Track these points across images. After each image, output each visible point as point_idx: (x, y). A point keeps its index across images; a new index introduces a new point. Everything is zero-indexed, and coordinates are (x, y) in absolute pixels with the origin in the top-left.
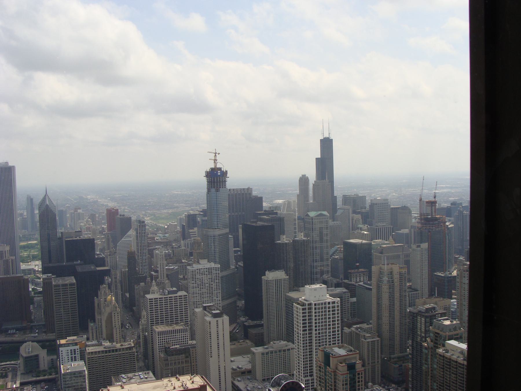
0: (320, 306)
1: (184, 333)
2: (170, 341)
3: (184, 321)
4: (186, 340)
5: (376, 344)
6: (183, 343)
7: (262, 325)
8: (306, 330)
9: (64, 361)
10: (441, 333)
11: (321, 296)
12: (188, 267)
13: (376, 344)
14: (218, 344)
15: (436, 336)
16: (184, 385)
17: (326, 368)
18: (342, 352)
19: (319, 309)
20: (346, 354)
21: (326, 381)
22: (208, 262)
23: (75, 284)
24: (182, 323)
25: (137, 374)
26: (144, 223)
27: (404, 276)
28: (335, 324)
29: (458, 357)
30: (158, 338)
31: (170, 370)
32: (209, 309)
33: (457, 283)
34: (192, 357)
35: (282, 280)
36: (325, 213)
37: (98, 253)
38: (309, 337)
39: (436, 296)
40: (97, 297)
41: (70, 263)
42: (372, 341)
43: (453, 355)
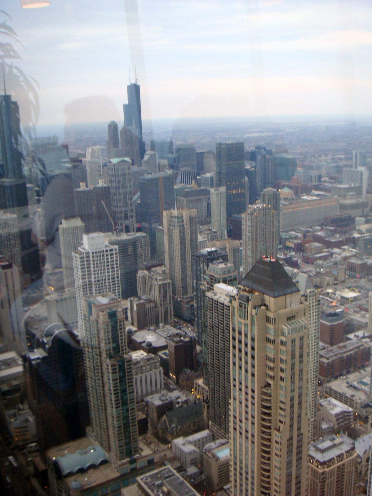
10: (215, 276)
13: (167, 286)
15: (212, 279)
17: (89, 316)
18: (104, 300)
20: (108, 302)
28: (112, 272)
29: (225, 299)
33: (242, 226)
36: (127, 159)
39: (226, 238)
42: (163, 284)
43: (220, 297)
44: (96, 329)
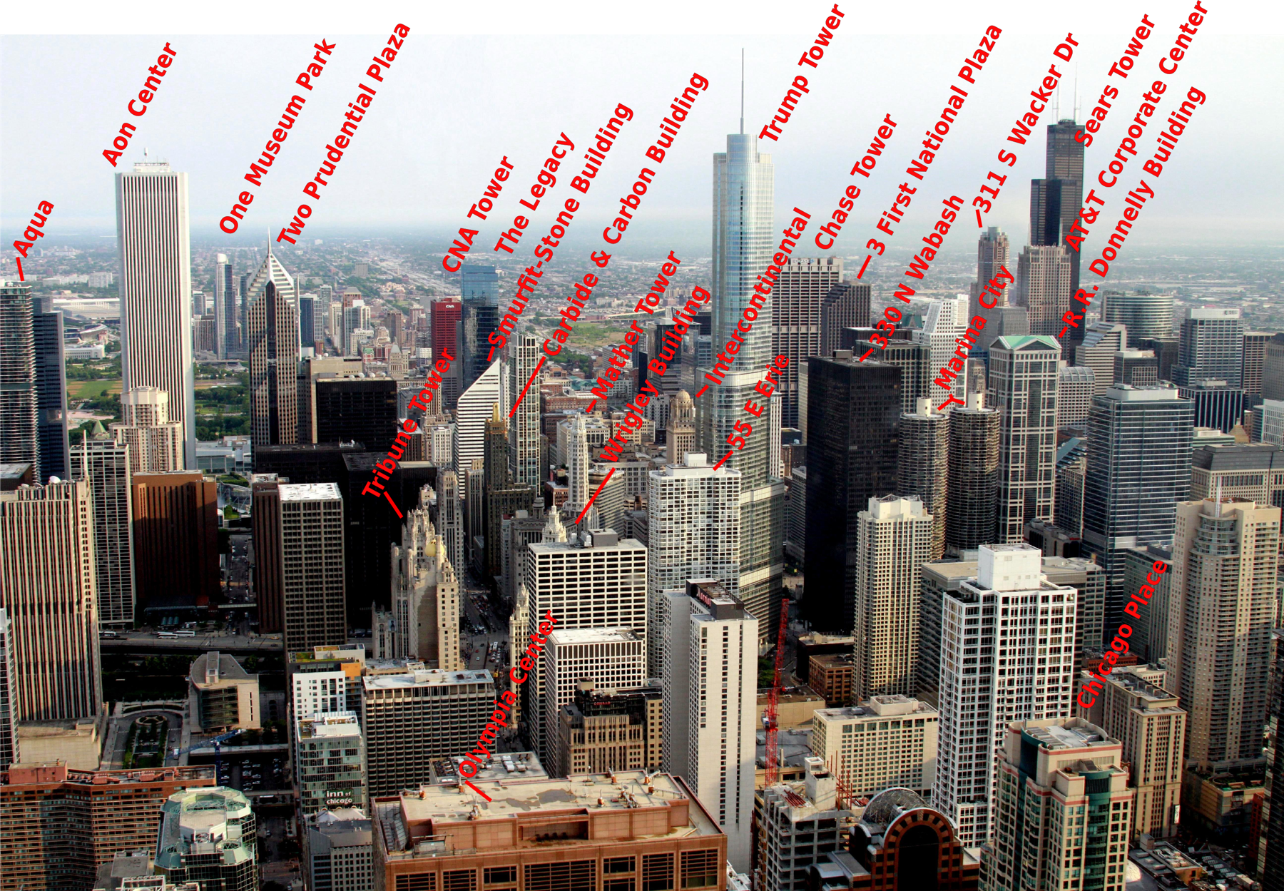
0: (1020, 606)
1: (631, 656)
2: (592, 674)
3: (633, 622)
4: (636, 674)
5: (1173, 725)
6: (626, 681)
7: (849, 648)
8: (974, 671)
9: (303, 709)
11: (1023, 577)
12: (651, 472)
13: (1173, 725)
14: (725, 691)
16: (627, 797)
19: (1015, 612)
21: (1020, 817)
22: (709, 461)
23: (339, 503)
24: (625, 628)
25: (496, 757)
26: (533, 344)
27: (1270, 537)
30: (560, 663)
31: (587, 755)
32: (705, 593)
34: (649, 721)
35: (914, 525)
37: (403, 420)
38: (980, 690)
40: (399, 544)
41: (327, 448)
44: (1041, 818)
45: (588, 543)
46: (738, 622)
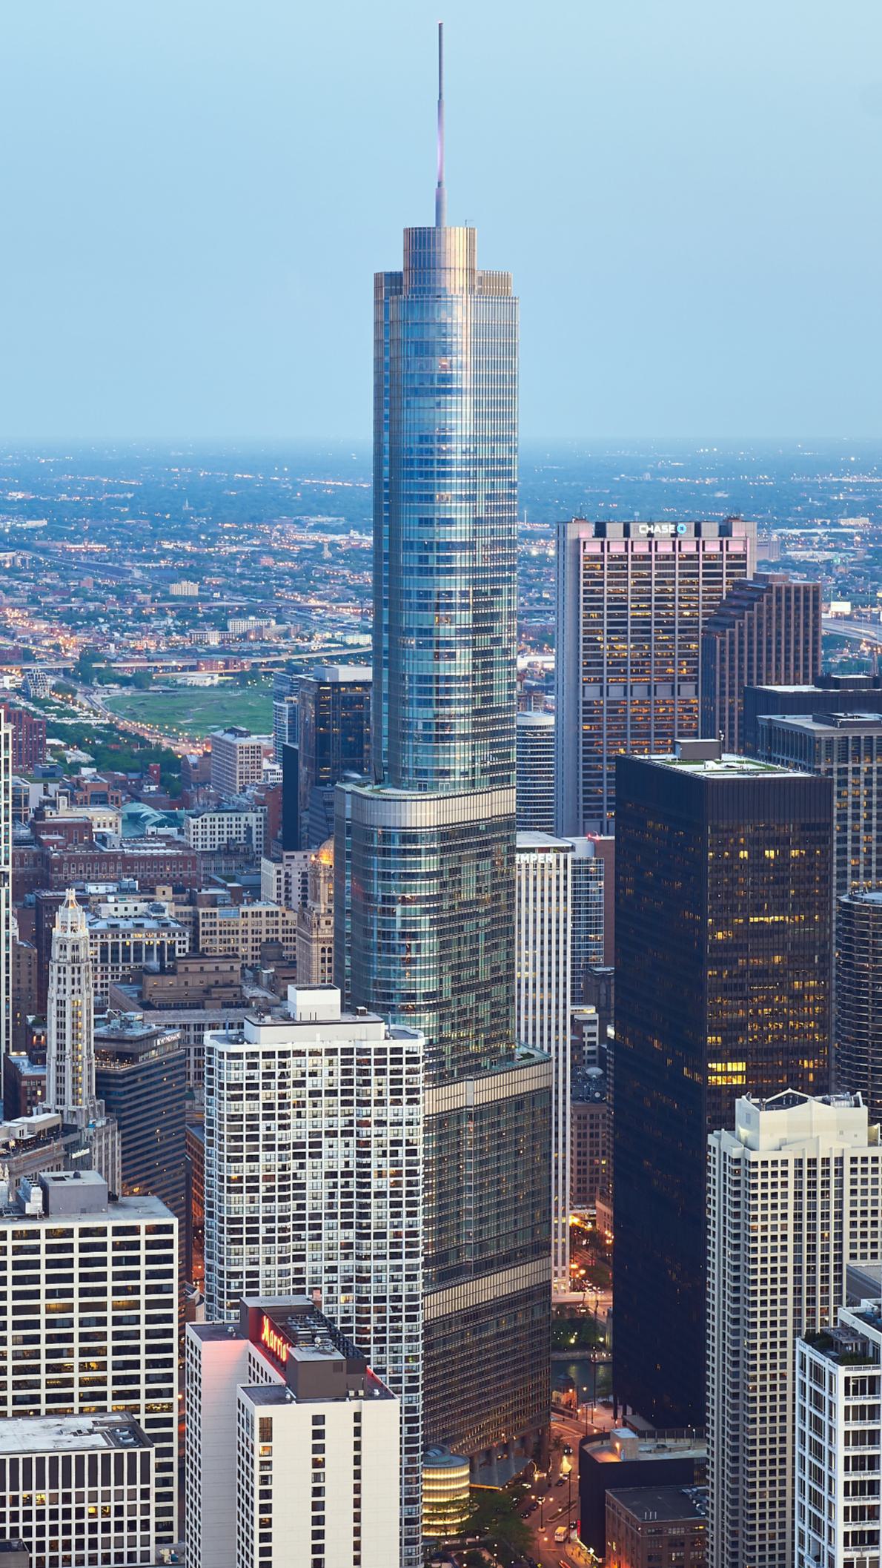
1: (126, 1487)
2: (28, 1531)
7: (691, 1471)
22: (348, 1006)
35: (847, 1166)
45: (34, 1205)
46: (350, 1406)
